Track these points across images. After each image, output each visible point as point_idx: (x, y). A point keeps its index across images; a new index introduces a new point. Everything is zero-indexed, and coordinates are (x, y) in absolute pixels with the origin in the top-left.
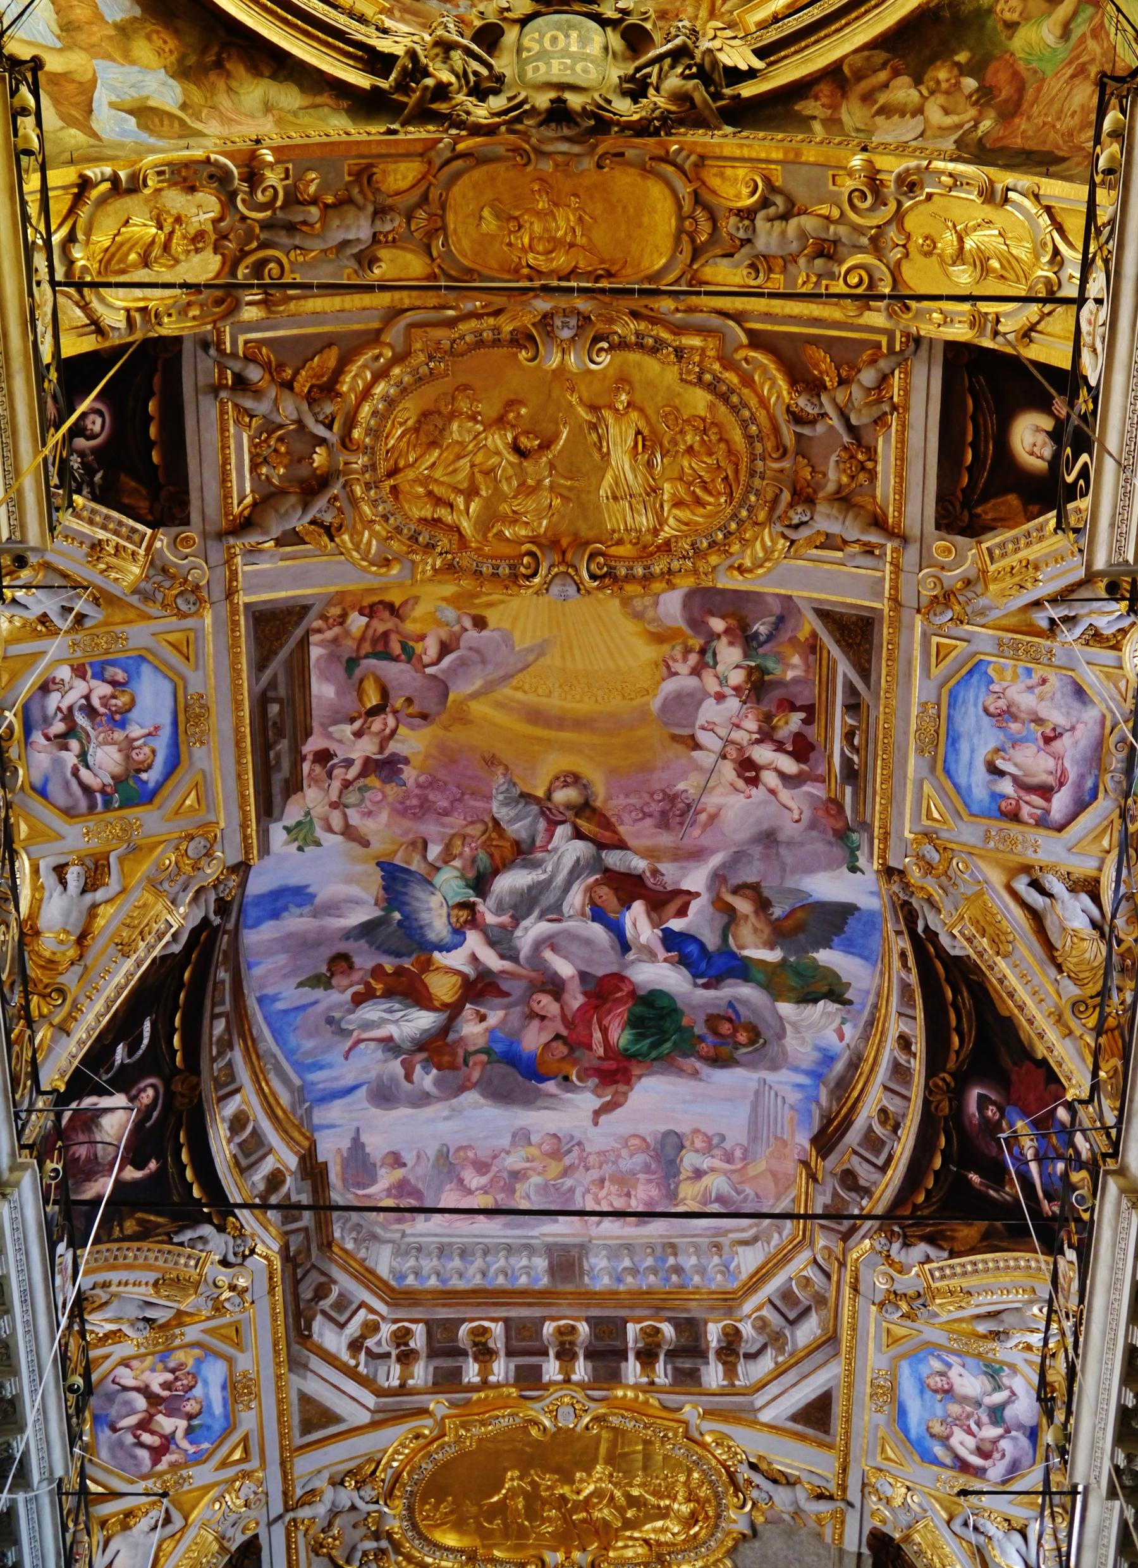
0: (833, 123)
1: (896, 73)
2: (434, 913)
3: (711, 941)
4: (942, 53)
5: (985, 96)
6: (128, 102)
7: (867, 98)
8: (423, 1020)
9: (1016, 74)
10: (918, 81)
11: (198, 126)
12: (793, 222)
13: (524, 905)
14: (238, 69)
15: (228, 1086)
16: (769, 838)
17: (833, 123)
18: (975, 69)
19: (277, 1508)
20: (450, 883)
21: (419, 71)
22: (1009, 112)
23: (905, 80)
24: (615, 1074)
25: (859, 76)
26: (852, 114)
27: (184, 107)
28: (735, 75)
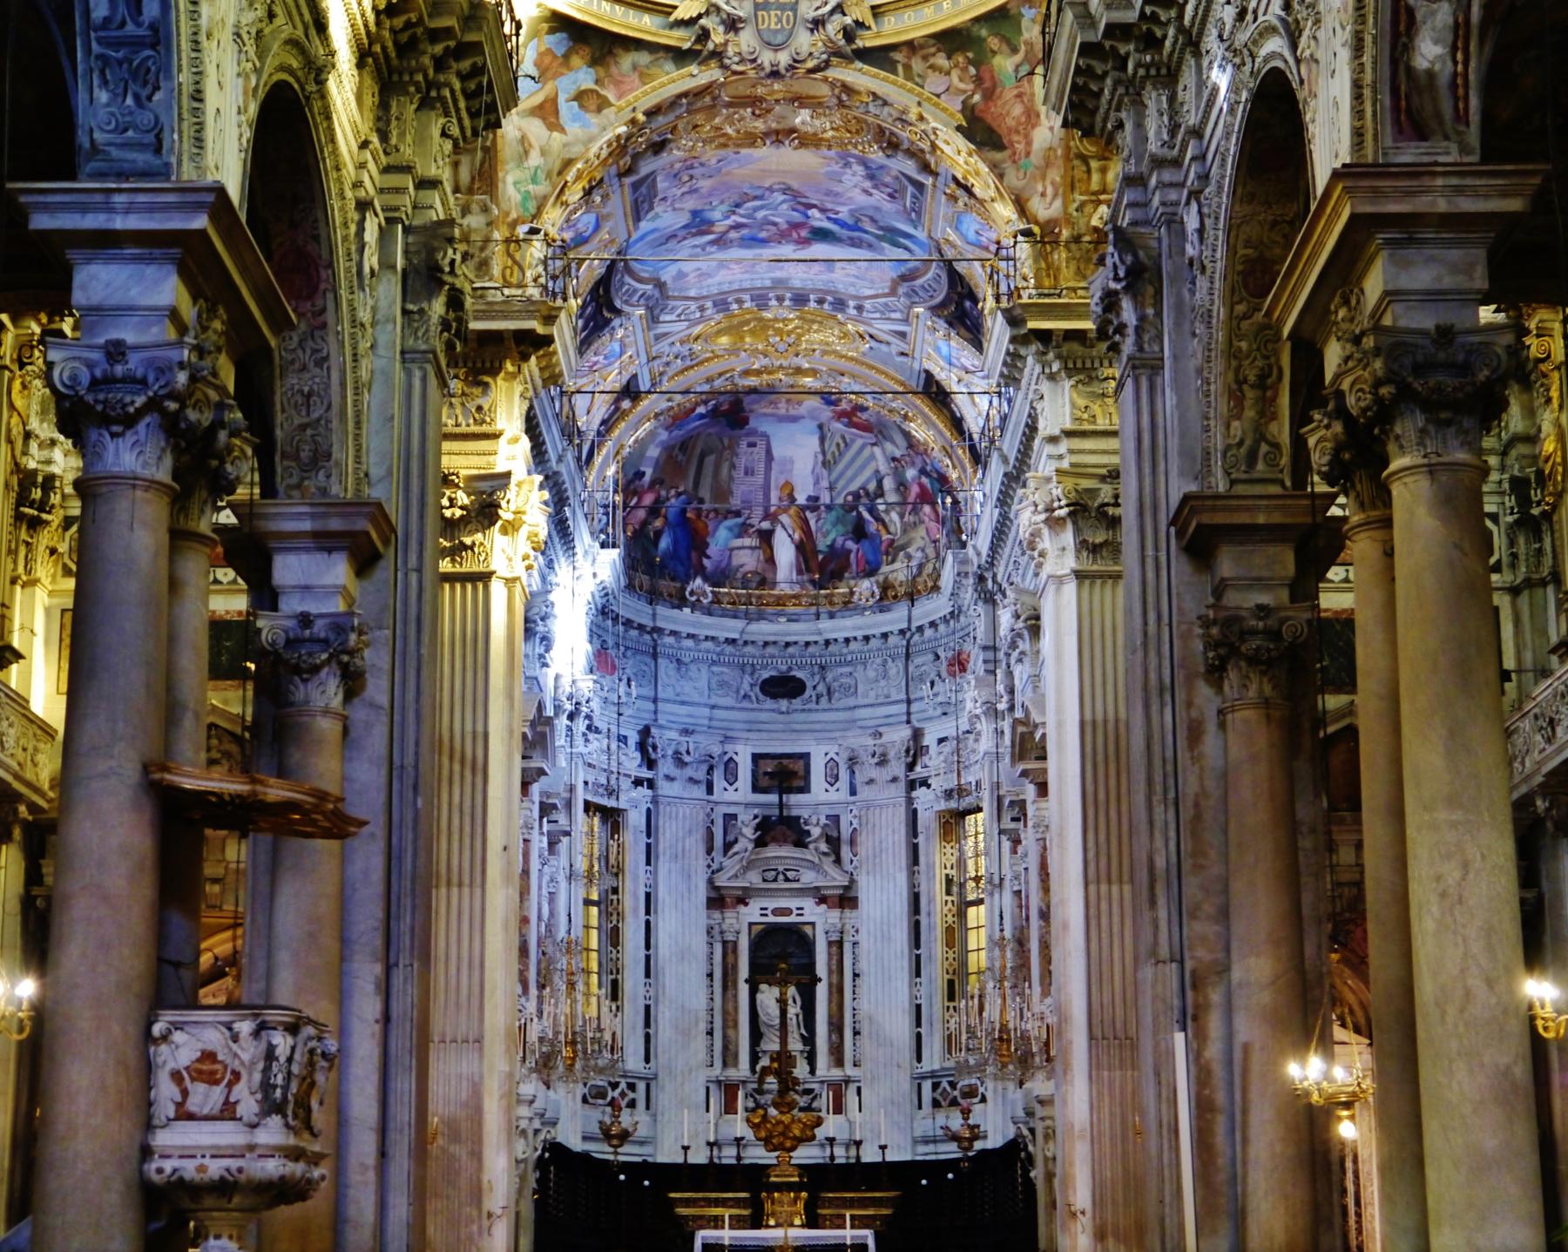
0: (908, 68)
1: (939, 50)
2: (716, 215)
3: (850, 222)
4: (962, 48)
5: (978, 80)
6: (573, 93)
7: (925, 58)
8: (711, 237)
9: (993, 77)
10: (949, 58)
11: (603, 92)
12: (886, 109)
13: (756, 209)
14: (621, 52)
15: (623, 284)
16: (877, 209)
17: (908, 68)
18: (976, 63)
19: (644, 359)
20: (724, 208)
21: (704, 35)
22: (989, 95)
23: (942, 54)
24: (804, 242)
25: (922, 47)
26: (917, 65)
27: (597, 82)
28: (860, 24)
